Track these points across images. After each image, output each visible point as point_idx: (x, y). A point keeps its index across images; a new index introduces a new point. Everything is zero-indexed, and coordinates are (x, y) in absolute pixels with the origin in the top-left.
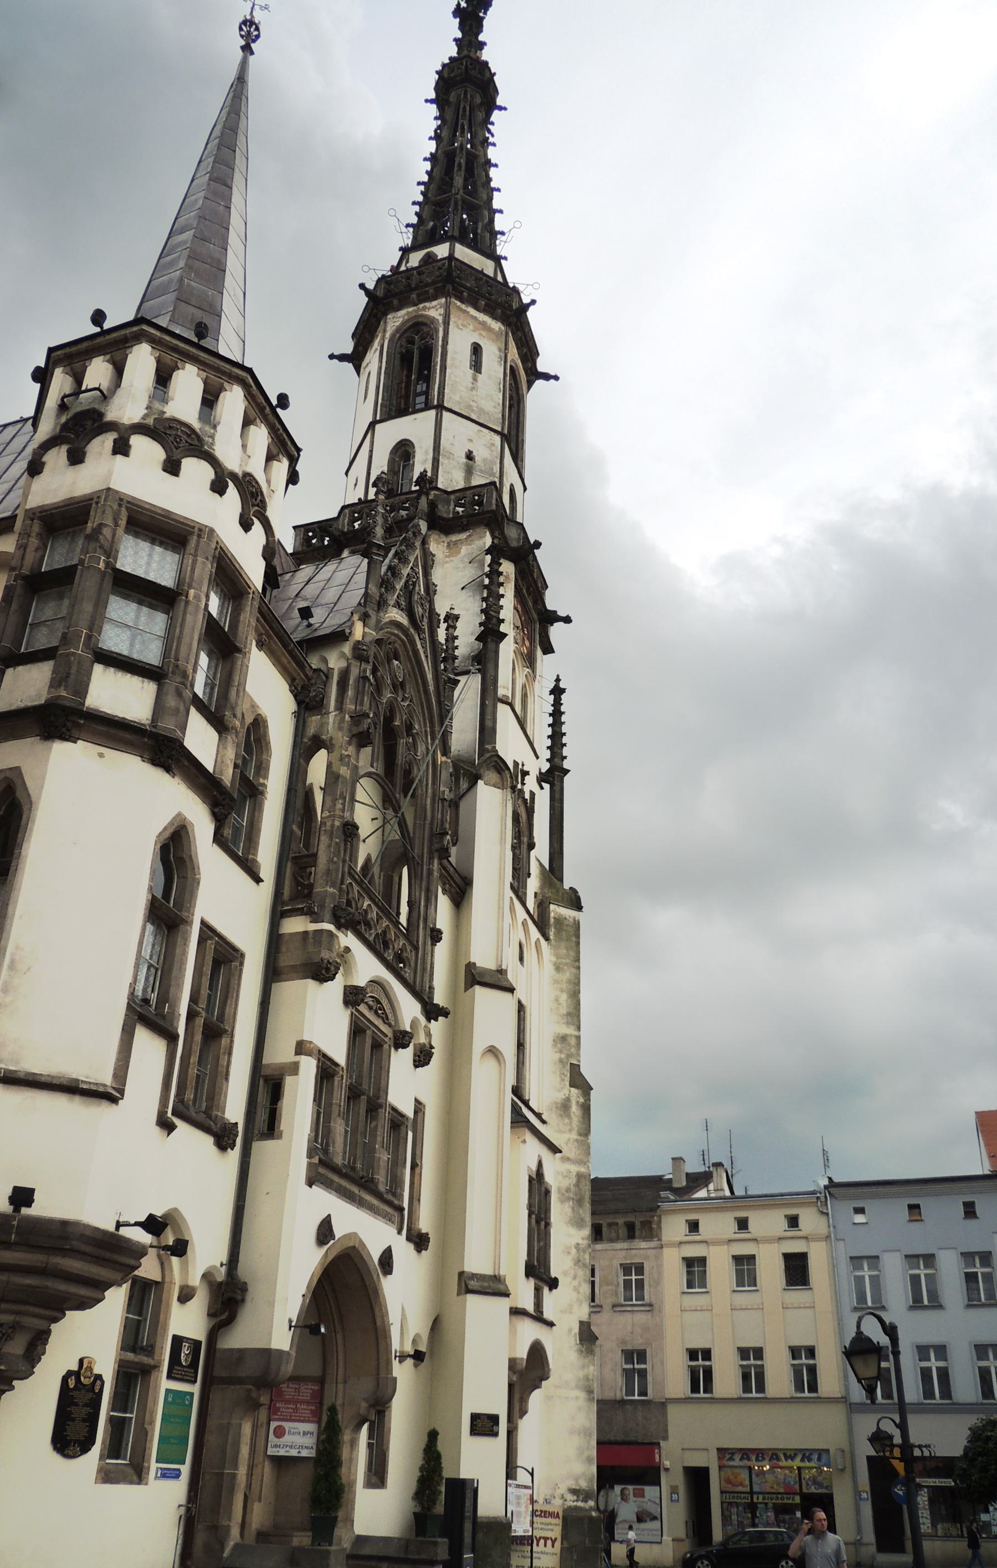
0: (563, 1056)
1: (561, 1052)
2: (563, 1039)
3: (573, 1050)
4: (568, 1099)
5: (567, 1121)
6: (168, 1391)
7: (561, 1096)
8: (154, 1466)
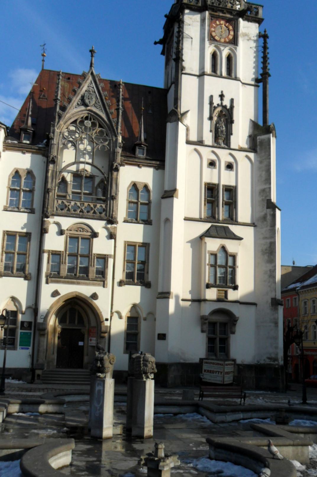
0: (264, 198)
1: (262, 196)
2: (263, 191)
3: (268, 194)
4: (266, 214)
5: (265, 223)
6: (21, 333)
7: (263, 214)
8: (18, 347)
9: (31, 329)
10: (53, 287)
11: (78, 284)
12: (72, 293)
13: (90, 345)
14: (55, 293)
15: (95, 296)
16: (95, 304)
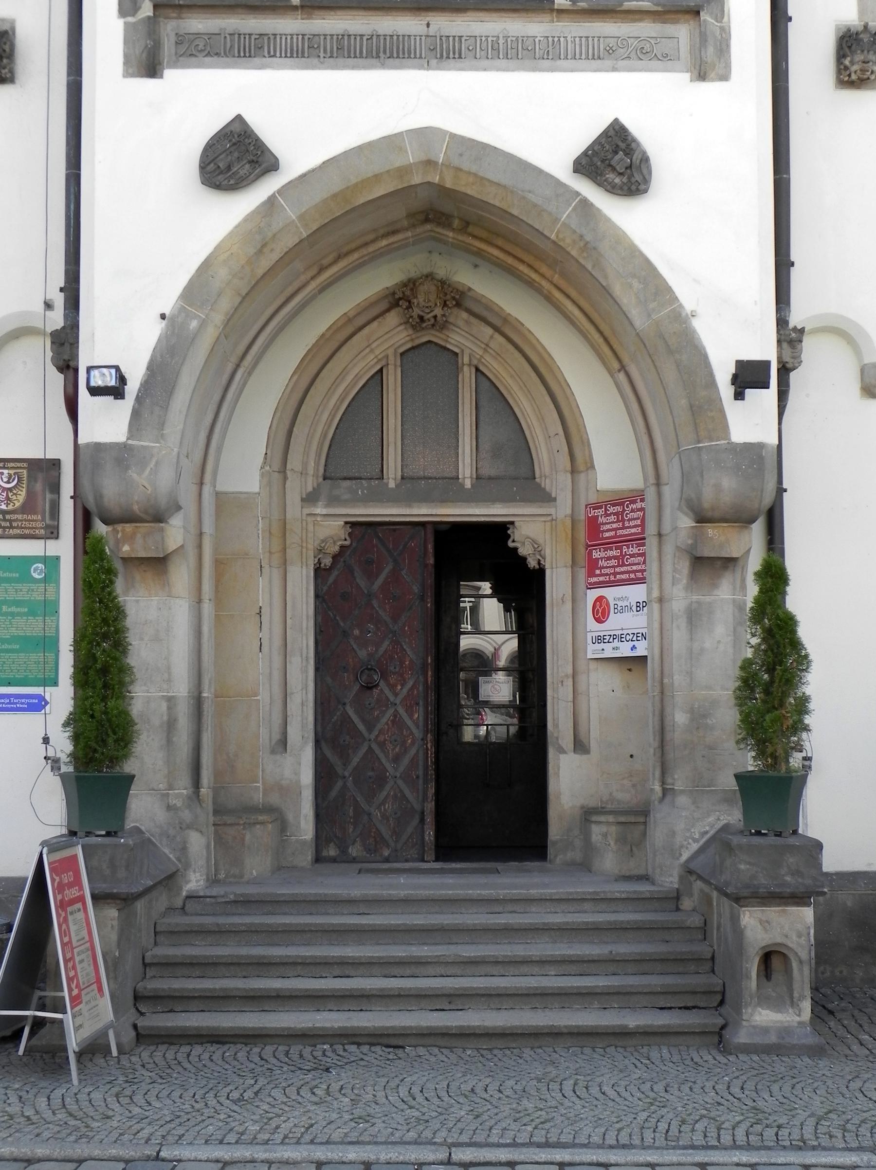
9: (53, 533)
10: (205, 96)
11: (446, 53)
12: (393, 142)
13: (592, 651)
14: (234, 157)
15: (616, 161)
16: (621, 240)
